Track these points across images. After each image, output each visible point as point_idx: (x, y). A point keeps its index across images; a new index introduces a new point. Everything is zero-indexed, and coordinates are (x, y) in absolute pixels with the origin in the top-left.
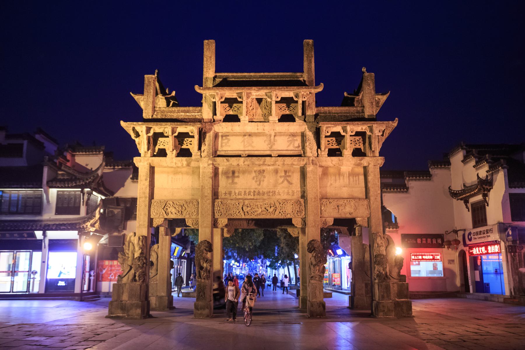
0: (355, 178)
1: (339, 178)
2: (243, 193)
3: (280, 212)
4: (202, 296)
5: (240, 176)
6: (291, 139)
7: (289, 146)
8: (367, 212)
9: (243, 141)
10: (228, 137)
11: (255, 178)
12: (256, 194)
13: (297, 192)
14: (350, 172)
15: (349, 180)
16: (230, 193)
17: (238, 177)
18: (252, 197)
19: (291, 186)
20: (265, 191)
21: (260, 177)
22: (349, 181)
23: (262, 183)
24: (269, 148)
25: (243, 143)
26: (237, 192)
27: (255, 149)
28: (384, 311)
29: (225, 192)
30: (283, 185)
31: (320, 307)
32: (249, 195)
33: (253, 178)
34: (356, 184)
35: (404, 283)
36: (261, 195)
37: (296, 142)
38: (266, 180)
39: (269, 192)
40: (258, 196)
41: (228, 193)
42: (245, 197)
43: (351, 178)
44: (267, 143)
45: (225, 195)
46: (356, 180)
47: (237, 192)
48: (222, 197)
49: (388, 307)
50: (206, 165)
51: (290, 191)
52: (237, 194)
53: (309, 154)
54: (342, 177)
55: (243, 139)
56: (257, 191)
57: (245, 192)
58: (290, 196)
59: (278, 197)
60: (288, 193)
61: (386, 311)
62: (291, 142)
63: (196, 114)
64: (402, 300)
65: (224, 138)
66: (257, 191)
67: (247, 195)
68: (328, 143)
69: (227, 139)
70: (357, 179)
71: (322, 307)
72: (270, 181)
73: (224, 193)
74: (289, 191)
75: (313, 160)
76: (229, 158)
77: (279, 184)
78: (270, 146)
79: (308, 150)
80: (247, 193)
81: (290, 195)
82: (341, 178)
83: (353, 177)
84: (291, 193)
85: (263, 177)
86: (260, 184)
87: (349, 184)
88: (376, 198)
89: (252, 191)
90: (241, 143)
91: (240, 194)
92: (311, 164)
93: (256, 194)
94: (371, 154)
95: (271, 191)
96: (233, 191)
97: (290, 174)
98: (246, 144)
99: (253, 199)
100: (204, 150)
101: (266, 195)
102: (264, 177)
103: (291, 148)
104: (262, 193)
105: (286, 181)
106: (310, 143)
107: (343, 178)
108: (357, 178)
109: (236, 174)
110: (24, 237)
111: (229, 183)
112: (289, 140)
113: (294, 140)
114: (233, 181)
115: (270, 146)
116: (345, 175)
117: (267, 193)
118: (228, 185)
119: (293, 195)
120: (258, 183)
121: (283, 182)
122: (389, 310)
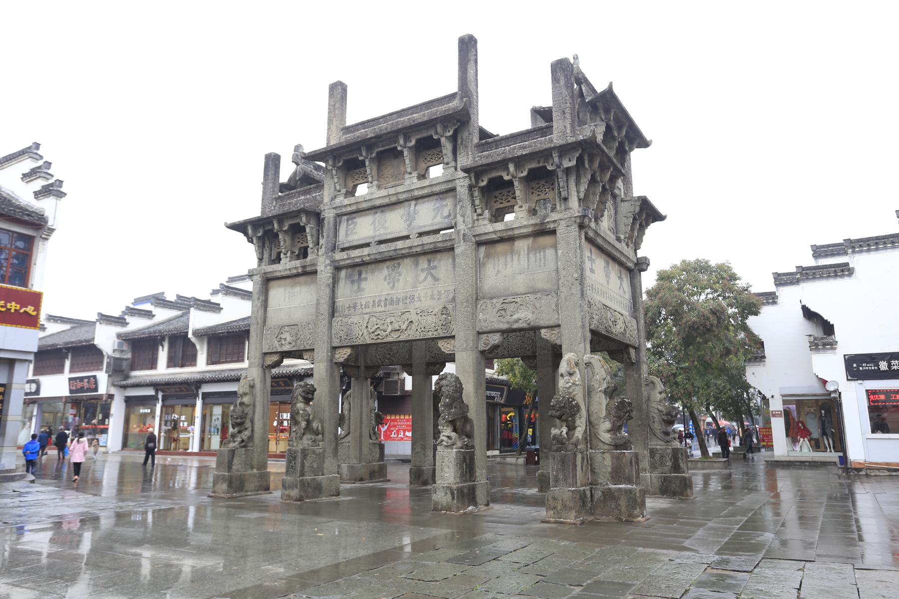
0: (538, 255)
1: (513, 258)
2: (371, 304)
3: (417, 330)
4: (292, 466)
5: (368, 277)
6: (438, 205)
7: (434, 217)
8: (556, 316)
9: (374, 222)
10: (355, 220)
11: (388, 278)
12: (388, 303)
14: (530, 246)
15: (528, 260)
16: (355, 307)
17: (366, 279)
18: (383, 309)
19: (437, 283)
20: (401, 296)
22: (528, 262)
25: (373, 225)
26: (364, 303)
27: (389, 231)
28: (555, 508)
31: (446, 494)
32: (378, 306)
33: (385, 279)
34: (540, 266)
35: (624, 453)
38: (402, 278)
39: (406, 298)
40: (391, 306)
42: (374, 309)
43: (532, 256)
44: (405, 219)
45: (349, 310)
46: (540, 259)
47: (364, 303)
49: (562, 500)
53: (461, 227)
54: (517, 256)
56: (389, 298)
57: (374, 301)
59: (417, 304)
60: (432, 297)
61: (559, 507)
62: (437, 210)
63: (318, 194)
64: (621, 486)
65: (350, 222)
66: (389, 298)
67: (376, 306)
68: (495, 200)
70: (542, 257)
71: (449, 495)
75: (464, 235)
78: (408, 222)
79: (460, 219)
80: (376, 302)
81: (435, 299)
82: (515, 258)
83: (536, 253)
84: (436, 297)
86: (394, 286)
87: (528, 268)
88: (570, 289)
89: (383, 299)
91: (367, 306)
92: (462, 242)
93: (388, 303)
94: (561, 206)
96: (359, 302)
97: (436, 263)
102: (400, 275)
103: (439, 219)
105: (429, 276)
106: (462, 207)
107: (519, 259)
108: (542, 254)
109: (363, 276)
110: (281, 386)
111: (355, 291)
113: (443, 206)
114: (359, 287)
115: (408, 222)
116: (522, 252)
117: (403, 300)
119: (439, 299)
120: (391, 285)
121: (426, 278)
122: (565, 506)
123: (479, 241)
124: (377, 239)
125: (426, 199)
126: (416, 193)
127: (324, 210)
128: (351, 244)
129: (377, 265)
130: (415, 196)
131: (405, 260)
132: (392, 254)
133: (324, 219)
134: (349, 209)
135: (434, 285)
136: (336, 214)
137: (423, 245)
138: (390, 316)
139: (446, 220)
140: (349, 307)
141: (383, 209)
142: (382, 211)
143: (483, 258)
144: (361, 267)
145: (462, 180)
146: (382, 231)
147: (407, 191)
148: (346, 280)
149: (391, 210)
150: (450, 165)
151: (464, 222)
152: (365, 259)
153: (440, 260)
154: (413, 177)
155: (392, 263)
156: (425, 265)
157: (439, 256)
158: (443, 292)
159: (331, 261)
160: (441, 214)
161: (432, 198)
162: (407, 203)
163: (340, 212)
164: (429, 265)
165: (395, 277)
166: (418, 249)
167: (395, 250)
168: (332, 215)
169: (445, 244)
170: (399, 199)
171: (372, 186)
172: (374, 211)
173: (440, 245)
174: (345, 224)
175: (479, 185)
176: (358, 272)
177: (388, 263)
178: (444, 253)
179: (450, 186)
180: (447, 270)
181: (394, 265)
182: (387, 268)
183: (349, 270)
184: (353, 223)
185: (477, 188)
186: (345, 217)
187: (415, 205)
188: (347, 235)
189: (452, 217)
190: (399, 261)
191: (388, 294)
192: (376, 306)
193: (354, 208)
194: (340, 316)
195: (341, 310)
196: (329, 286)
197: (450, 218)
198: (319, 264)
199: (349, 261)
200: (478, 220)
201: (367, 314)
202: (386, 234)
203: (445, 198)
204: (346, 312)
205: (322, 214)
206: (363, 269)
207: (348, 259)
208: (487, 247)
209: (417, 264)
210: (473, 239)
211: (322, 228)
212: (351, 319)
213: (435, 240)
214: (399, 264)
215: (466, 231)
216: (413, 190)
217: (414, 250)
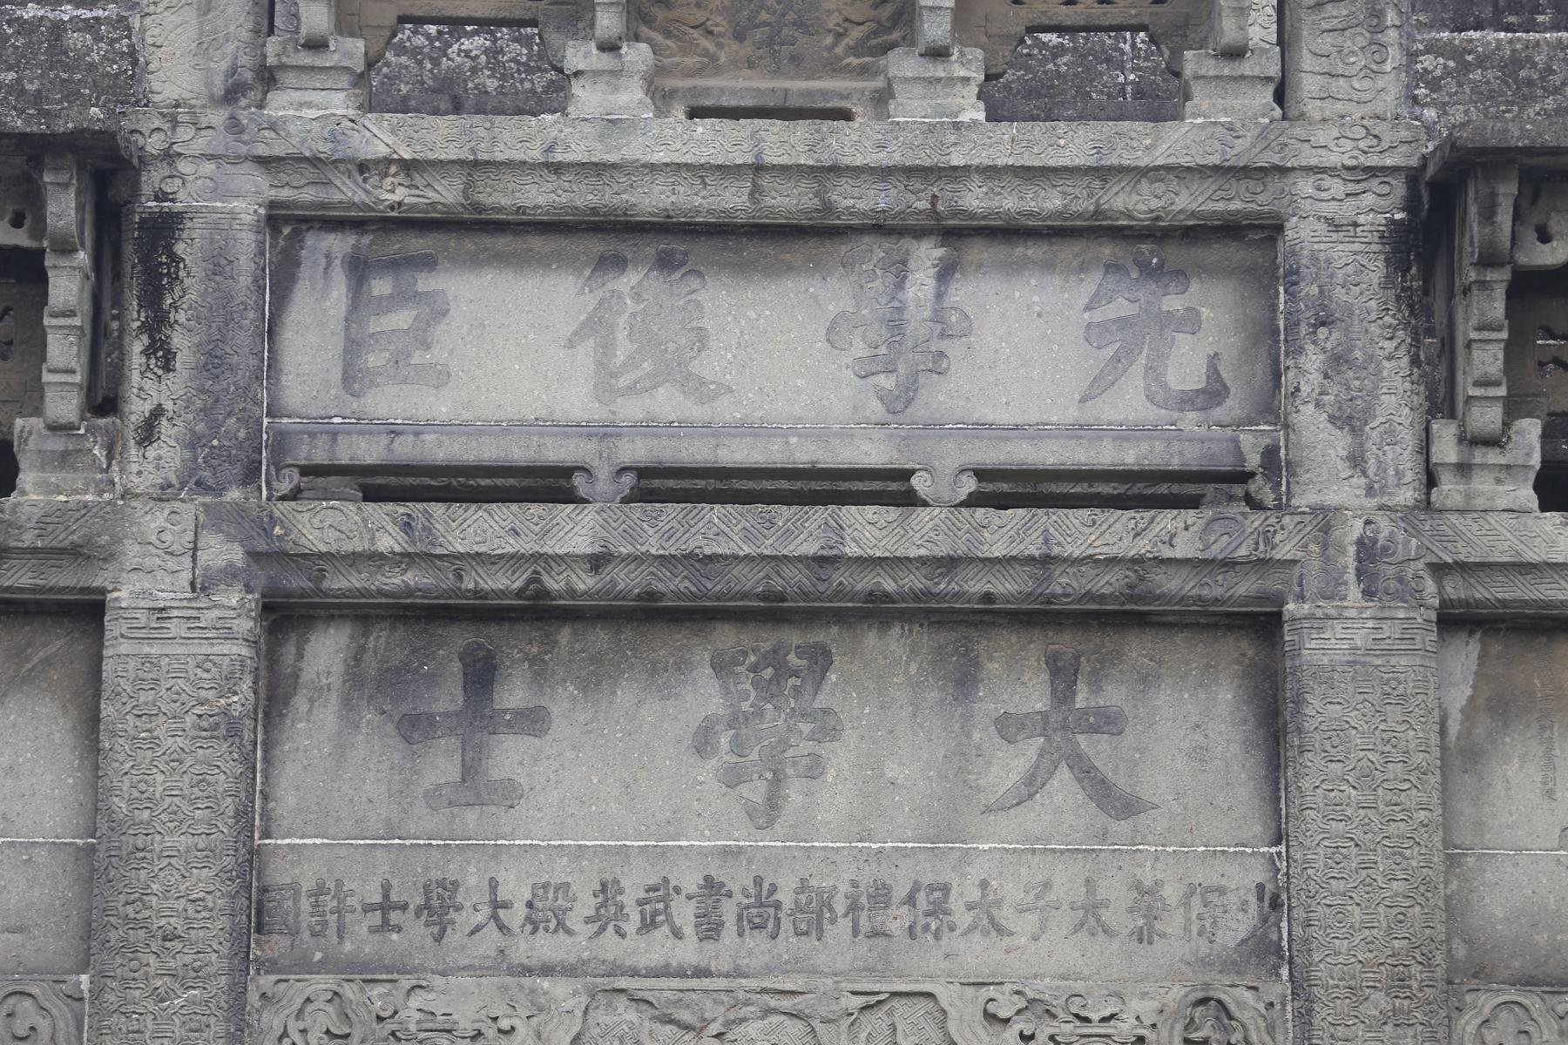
2: (586, 904)
5: (555, 711)
6: (1121, 307)
7: (1098, 386)
9: (595, 326)
10: (426, 282)
11: (724, 741)
13: (1186, 905)
17: (533, 721)
18: (688, 952)
19: (1122, 827)
20: (839, 882)
21: (773, 720)
23: (794, 794)
24: (876, 409)
26: (516, 889)
27: (727, 411)
29: (386, 889)
30: (1034, 817)
32: (648, 925)
33: (703, 743)
36: (786, 924)
37: (1184, 342)
38: (840, 757)
39: (881, 896)
40: (757, 942)
41: (420, 900)
42: (611, 947)
44: (860, 350)
45: (386, 927)
47: (516, 889)
48: (348, 947)
50: (171, 587)
51: (1115, 891)
52: (520, 911)
55: (590, 301)
56: (737, 880)
58: (1115, 945)
59: (977, 953)
60: (1090, 919)
65: (381, 286)
66: (737, 880)
67: (631, 927)
69: (418, 297)
72: (892, 770)
73: (368, 908)
74: (1101, 894)
75: (1367, 551)
76: (438, 509)
77: (988, 810)
78: (887, 382)
80: (628, 899)
85: (805, 728)
86: (773, 804)
89: (691, 882)
90: (570, 344)
92: (1354, 592)
93: (729, 911)
95: (901, 891)
96: (473, 880)
97: (1114, 695)
98: (620, 356)
99: (702, 972)
100: (158, 412)
101: (844, 924)
104: (798, 908)
105: (1064, 774)
106: (1338, 361)
109: (513, 694)
112: (1097, 316)
114: (470, 771)
115: (887, 382)
117: (853, 908)
118: (420, 808)
119: (1143, 937)
120: (755, 791)
121: (1032, 785)
123: (1465, 603)
124: (637, 451)
125: (1034, 250)
126: (974, 199)
127: (169, 156)
128: (405, 450)
129: (627, 634)
130: (956, 213)
131: (871, 639)
132: (793, 579)
133: (166, 227)
134: (394, 193)
135: (1104, 836)
136: (272, 205)
137: (1047, 560)
138: (769, 1011)
139: (1190, 421)
140: (386, 907)
141: (679, 246)
142: (666, 263)
143: (1469, 712)
144: (493, 630)
145: (1336, 187)
146: (667, 403)
147: (909, 171)
148: (347, 703)
149: (744, 268)
150: (1247, 67)
151: (1356, 460)
152: (554, 583)
153: (1147, 680)
154: (951, 81)
155: (765, 639)
156: (1033, 695)
157: (1138, 649)
158: (1172, 893)
159: (254, 555)
160: (1154, 371)
161: (1069, 251)
162: (878, 249)
163: (308, 195)
164: (1063, 693)
165: (784, 744)
166: (1006, 586)
167: (822, 561)
168: (247, 209)
169: (1216, 588)
170: (828, 208)
171: (615, 73)
172: (596, 246)
173: (1173, 584)
174: (339, 290)
175: (1523, 259)
176: (467, 658)
177: (726, 637)
178: (1179, 638)
179: (1236, 202)
180: (1199, 754)
181: (776, 658)
182: (721, 667)
183: (380, 638)
184: (404, 297)
185: (1505, 274)
186: (339, 244)
187: (945, 273)
188: (352, 378)
189: (1232, 407)
190: (818, 636)
191: (726, 852)
192: (631, 927)
193: (445, 193)
194: (305, 966)
195: (306, 919)
196: (233, 732)
197: (1219, 413)
198: (132, 553)
199: (412, 578)
200: (1464, 469)
201: (547, 970)
202: (707, 428)
203: (1181, 274)
204: (361, 939)
205: (152, 179)
206: (514, 646)
207: (407, 559)
208: (1496, 648)
209: (965, 681)
210: (1430, 586)
211: (153, 297)
212: (417, 1001)
213: (1143, 546)
214: (821, 660)
215: (1384, 526)
216: (957, 174)
217: (976, 584)
